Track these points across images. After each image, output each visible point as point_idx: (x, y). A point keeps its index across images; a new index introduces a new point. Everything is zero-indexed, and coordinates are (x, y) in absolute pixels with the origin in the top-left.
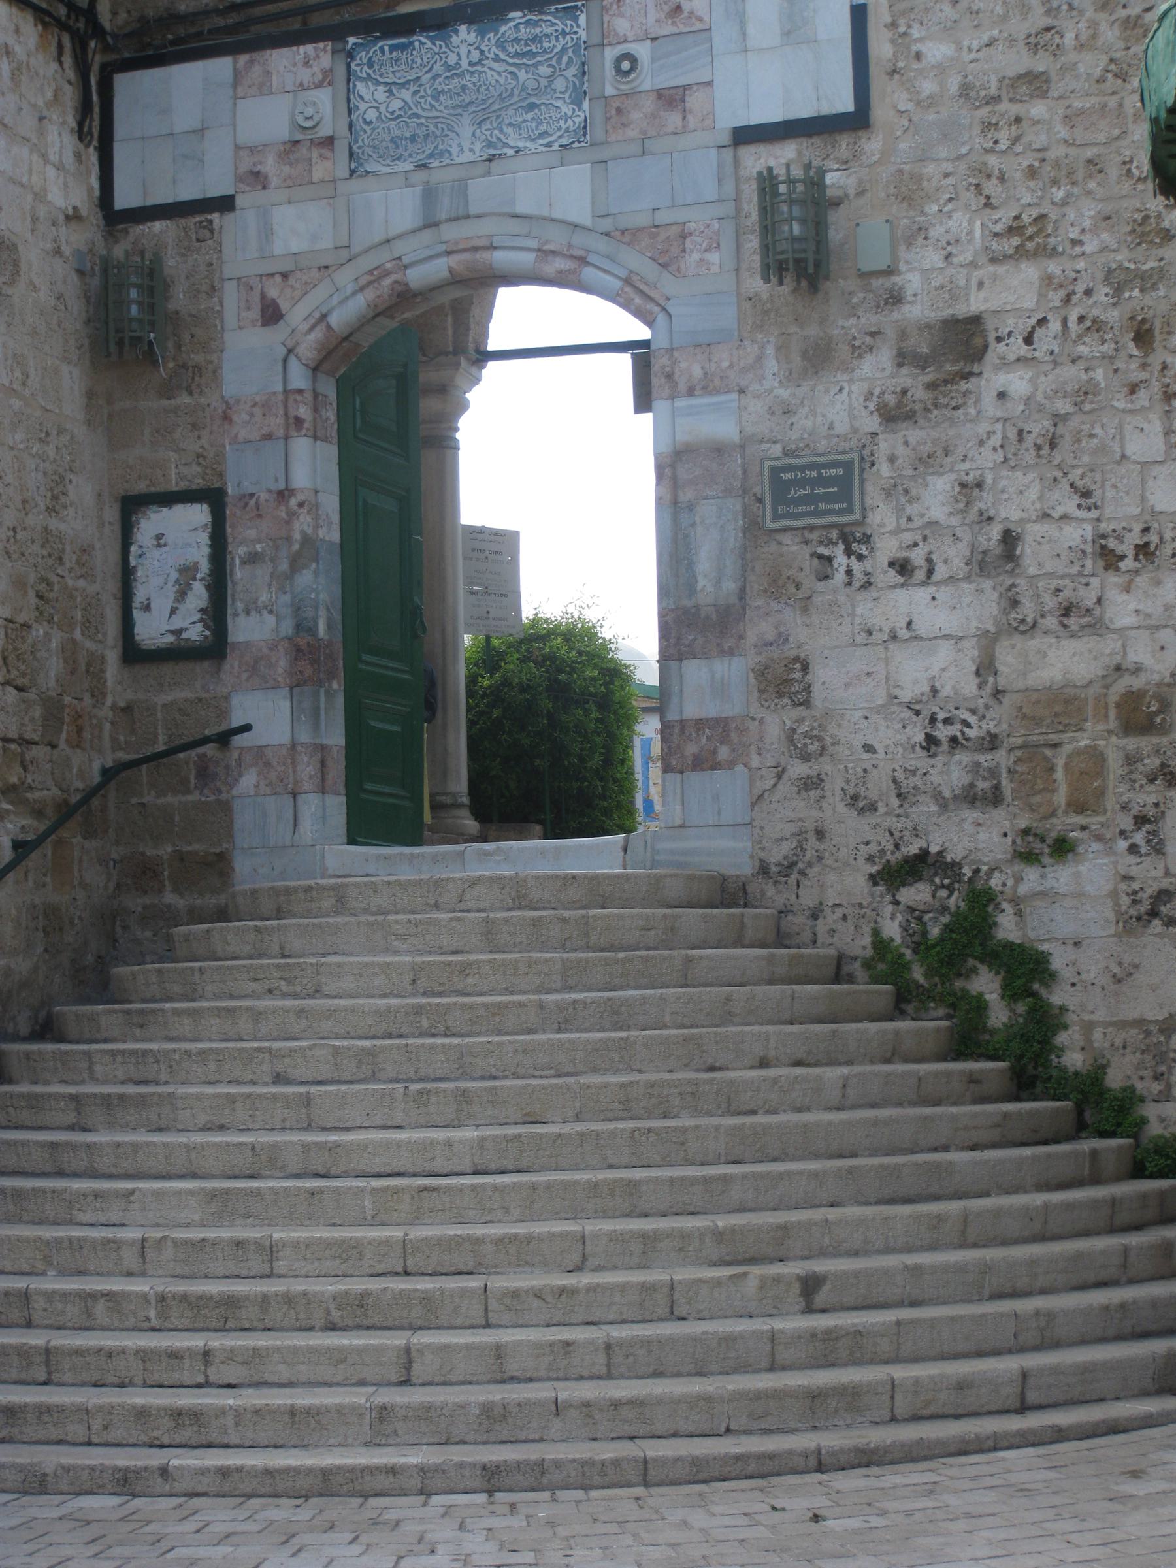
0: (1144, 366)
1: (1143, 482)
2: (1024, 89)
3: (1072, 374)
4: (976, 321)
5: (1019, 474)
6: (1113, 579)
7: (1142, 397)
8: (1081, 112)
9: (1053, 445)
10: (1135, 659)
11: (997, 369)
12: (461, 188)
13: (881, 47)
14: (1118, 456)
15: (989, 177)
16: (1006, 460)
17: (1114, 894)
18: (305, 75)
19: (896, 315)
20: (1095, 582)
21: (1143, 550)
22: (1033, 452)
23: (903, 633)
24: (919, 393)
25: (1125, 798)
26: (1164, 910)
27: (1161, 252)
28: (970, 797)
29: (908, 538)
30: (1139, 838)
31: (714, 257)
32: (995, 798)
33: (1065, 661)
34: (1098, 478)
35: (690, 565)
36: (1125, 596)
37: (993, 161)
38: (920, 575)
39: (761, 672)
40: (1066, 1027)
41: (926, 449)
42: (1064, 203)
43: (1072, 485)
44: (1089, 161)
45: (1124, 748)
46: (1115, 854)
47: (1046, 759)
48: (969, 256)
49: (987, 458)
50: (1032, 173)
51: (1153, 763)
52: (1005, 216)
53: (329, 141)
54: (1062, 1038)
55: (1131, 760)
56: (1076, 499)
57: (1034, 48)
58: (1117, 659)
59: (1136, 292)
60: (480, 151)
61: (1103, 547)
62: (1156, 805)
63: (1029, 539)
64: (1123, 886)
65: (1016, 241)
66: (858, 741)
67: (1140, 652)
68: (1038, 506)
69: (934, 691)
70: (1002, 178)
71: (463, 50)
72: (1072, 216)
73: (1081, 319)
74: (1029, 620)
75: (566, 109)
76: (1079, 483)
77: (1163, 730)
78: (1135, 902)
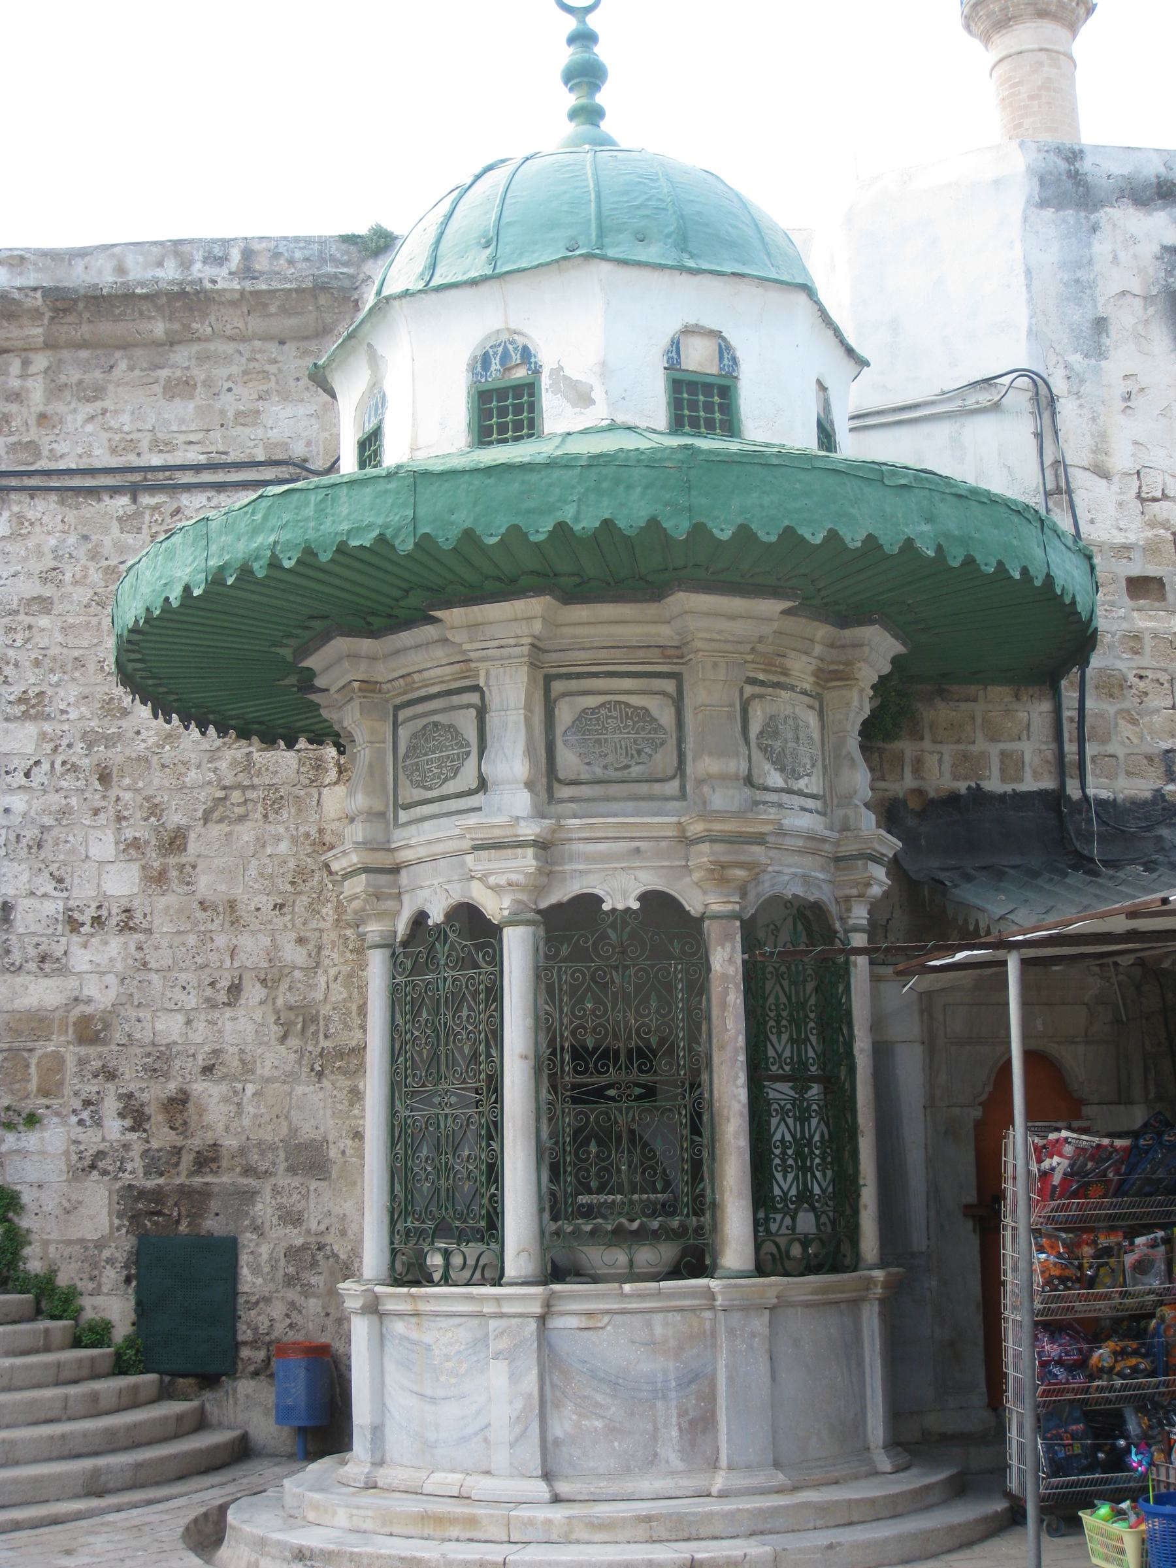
0: (104, 797)
1: (100, 875)
2: (35, 607)
5: (16, 864)
6: (75, 938)
8: (73, 626)
9: (40, 846)
10: (88, 993)
14: (83, 857)
15: (8, 663)
16: (7, 854)
17: (67, 1153)
20: (63, 940)
21: (97, 920)
22: (26, 850)
25: (76, 1088)
26: (100, 1164)
27: (119, 723)
30: (85, 1115)
34: (69, 870)
36: (83, 951)
37: (11, 653)
40: (30, 1243)
42: (57, 685)
43: (51, 874)
44: (76, 659)
45: (78, 1053)
46: (69, 1125)
47: (25, 1059)
50: (37, 663)
54: (27, 1251)
55: (82, 1062)
56: (54, 884)
57: (44, 581)
58: (76, 993)
59: (102, 748)
61: (70, 917)
62: (98, 1093)
63: (20, 909)
64: (73, 1148)
65: (23, 708)
67: (91, 989)
68: (27, 887)
70: (16, 665)
72: (62, 693)
73: (64, 763)
74: (17, 963)
76: (56, 873)
77: (105, 1042)
78: (80, 1158)
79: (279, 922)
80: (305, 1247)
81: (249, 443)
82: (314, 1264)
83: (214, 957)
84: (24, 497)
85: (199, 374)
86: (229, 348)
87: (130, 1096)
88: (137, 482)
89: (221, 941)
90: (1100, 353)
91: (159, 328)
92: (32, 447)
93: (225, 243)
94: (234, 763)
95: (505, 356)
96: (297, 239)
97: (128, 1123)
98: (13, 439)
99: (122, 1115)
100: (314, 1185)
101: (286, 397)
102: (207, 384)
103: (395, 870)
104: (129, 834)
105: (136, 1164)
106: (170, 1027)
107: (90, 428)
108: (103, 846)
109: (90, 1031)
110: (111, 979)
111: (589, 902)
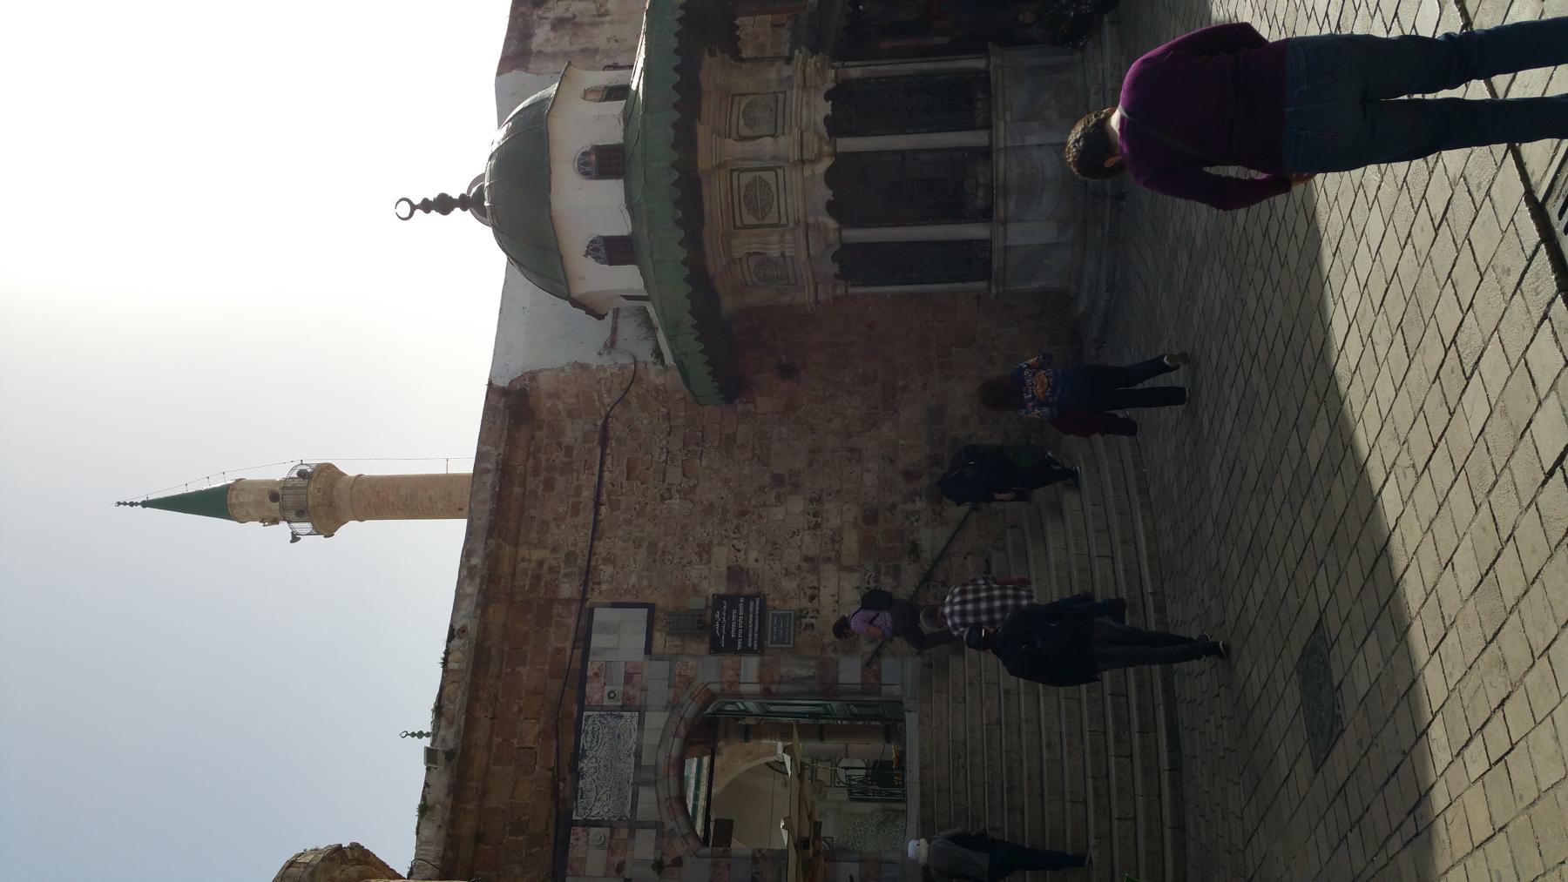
13: (628, 599)
18: (583, 840)
21: (815, 515)
33: (851, 542)
50: (682, 548)
52: (695, 558)
53: (613, 829)
85: (544, 474)
86: (531, 460)
90: (596, 51)
91: (517, 490)
92: (570, 557)
95: (586, 164)
99: (914, 502)
103: (807, 225)
108: (778, 513)
109: (870, 517)
111: (827, 120)
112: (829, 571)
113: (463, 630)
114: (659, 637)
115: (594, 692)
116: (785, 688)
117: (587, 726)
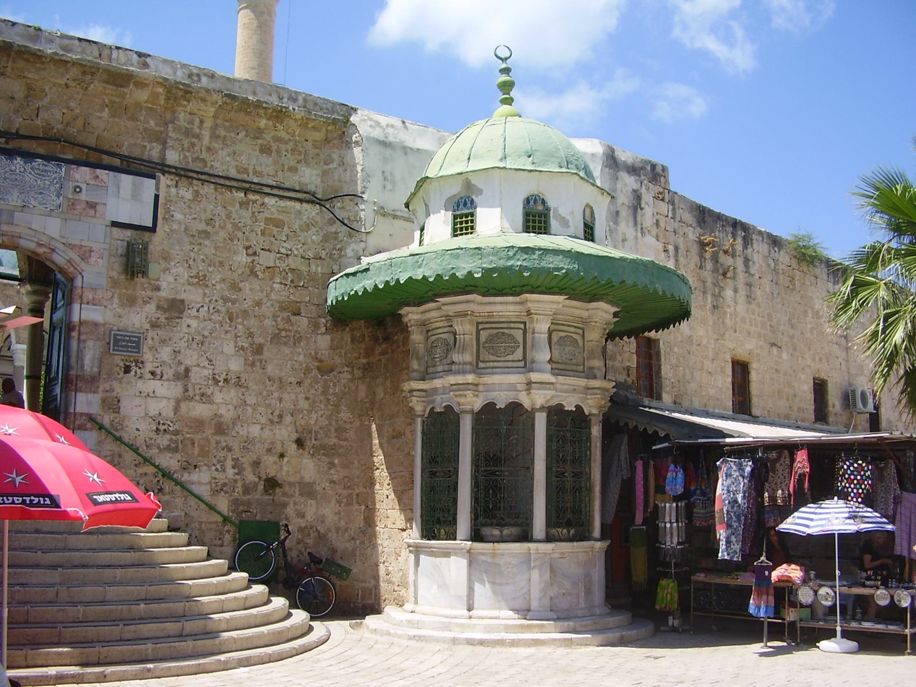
2: (203, 235)
3: (210, 325)
4: (183, 301)
7: (229, 335)
8: (219, 247)
11: (187, 317)
12: (12, 213)
17: (210, 483)
19: (158, 294)
21: (226, 380)
23: (151, 395)
24: (163, 319)
28: (168, 448)
29: (156, 365)
30: (218, 467)
31: (100, 261)
32: (176, 450)
33: (201, 410)
35: (82, 360)
38: (159, 377)
39: (104, 401)
41: (163, 338)
48: (182, 281)
49: (182, 344)
51: (224, 444)
55: (218, 443)
60: (20, 203)
66: (134, 427)
67: (222, 411)
69: (160, 414)
71: (18, 166)
75: (54, 198)
77: (227, 434)
79: (298, 389)
80: (306, 528)
81: (291, 180)
82: (309, 535)
83: (273, 402)
84: (199, 183)
85: (274, 146)
87: (237, 459)
88: (249, 187)
89: (276, 395)
91: (263, 123)
92: (204, 161)
93: (296, 93)
94: (283, 319)
96: (324, 99)
97: (236, 471)
98: (195, 156)
99: (233, 467)
100: (310, 501)
101: (307, 164)
102: (278, 151)
104: (240, 344)
105: (239, 489)
106: (255, 430)
107: (228, 158)
108: (229, 348)
109: (221, 429)
110: (230, 407)
112: (176, 390)
113: (146, 65)
114: (129, 233)
115: (83, 174)
116: (74, 344)
117: (51, 166)
